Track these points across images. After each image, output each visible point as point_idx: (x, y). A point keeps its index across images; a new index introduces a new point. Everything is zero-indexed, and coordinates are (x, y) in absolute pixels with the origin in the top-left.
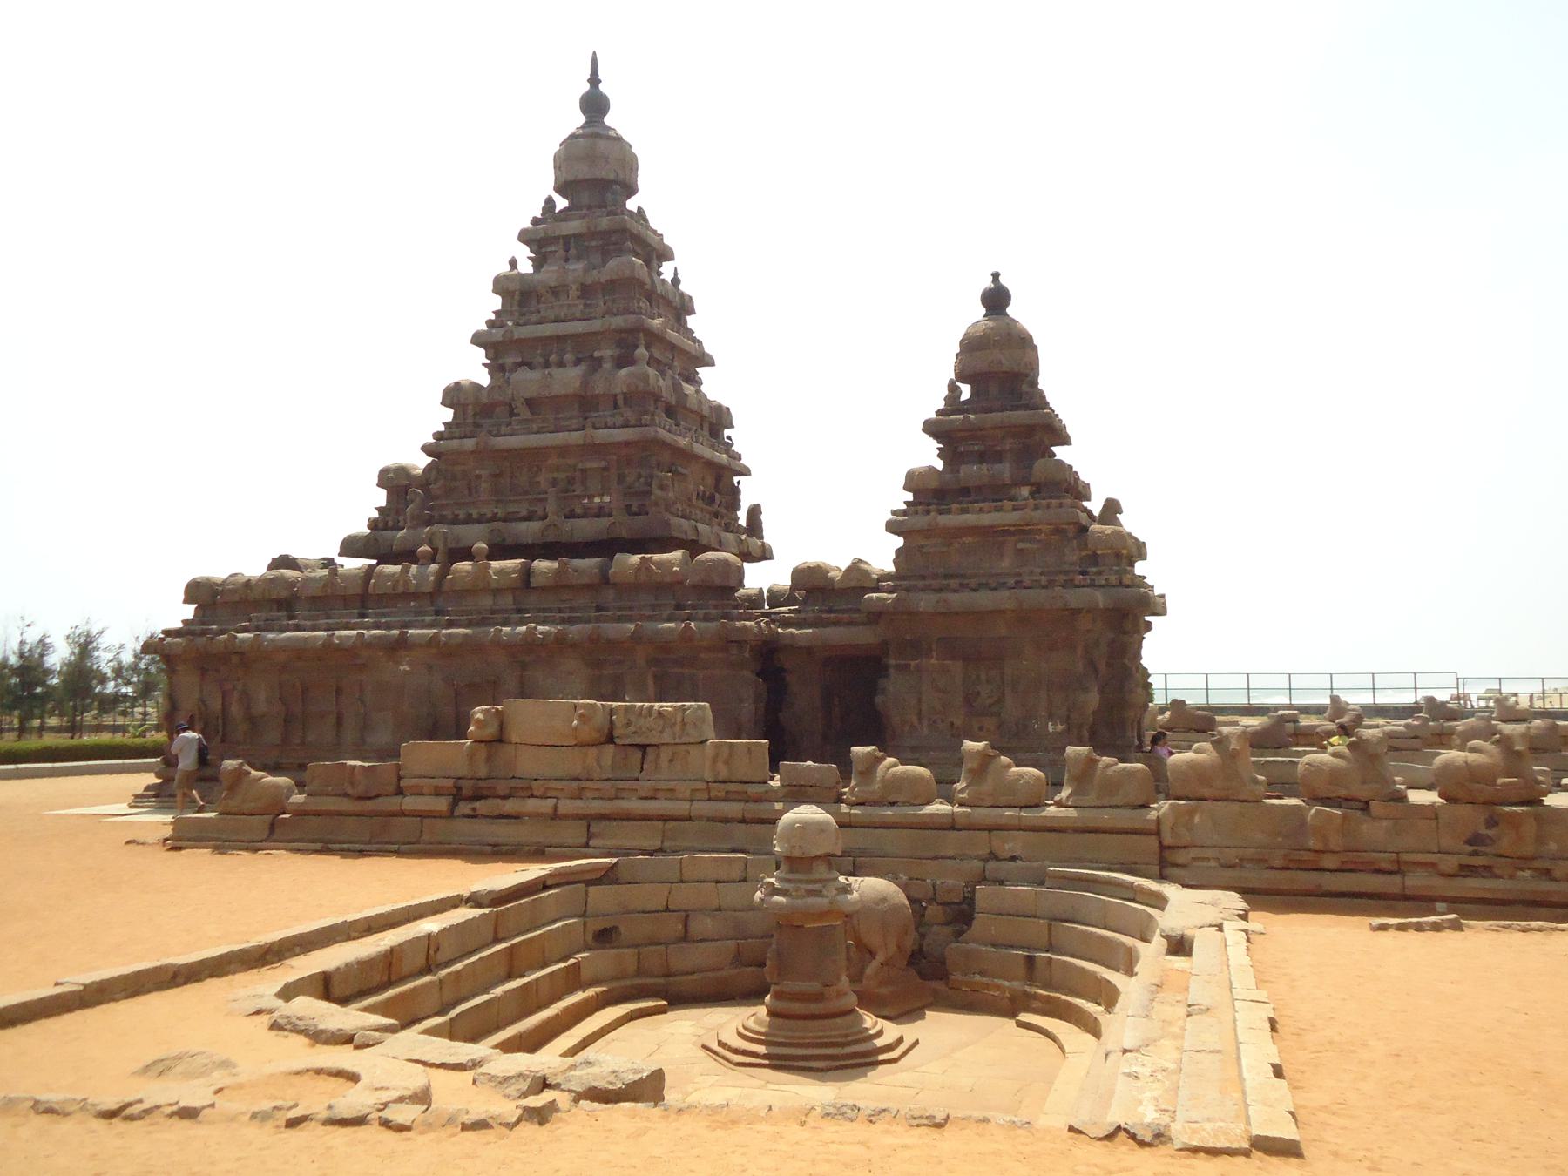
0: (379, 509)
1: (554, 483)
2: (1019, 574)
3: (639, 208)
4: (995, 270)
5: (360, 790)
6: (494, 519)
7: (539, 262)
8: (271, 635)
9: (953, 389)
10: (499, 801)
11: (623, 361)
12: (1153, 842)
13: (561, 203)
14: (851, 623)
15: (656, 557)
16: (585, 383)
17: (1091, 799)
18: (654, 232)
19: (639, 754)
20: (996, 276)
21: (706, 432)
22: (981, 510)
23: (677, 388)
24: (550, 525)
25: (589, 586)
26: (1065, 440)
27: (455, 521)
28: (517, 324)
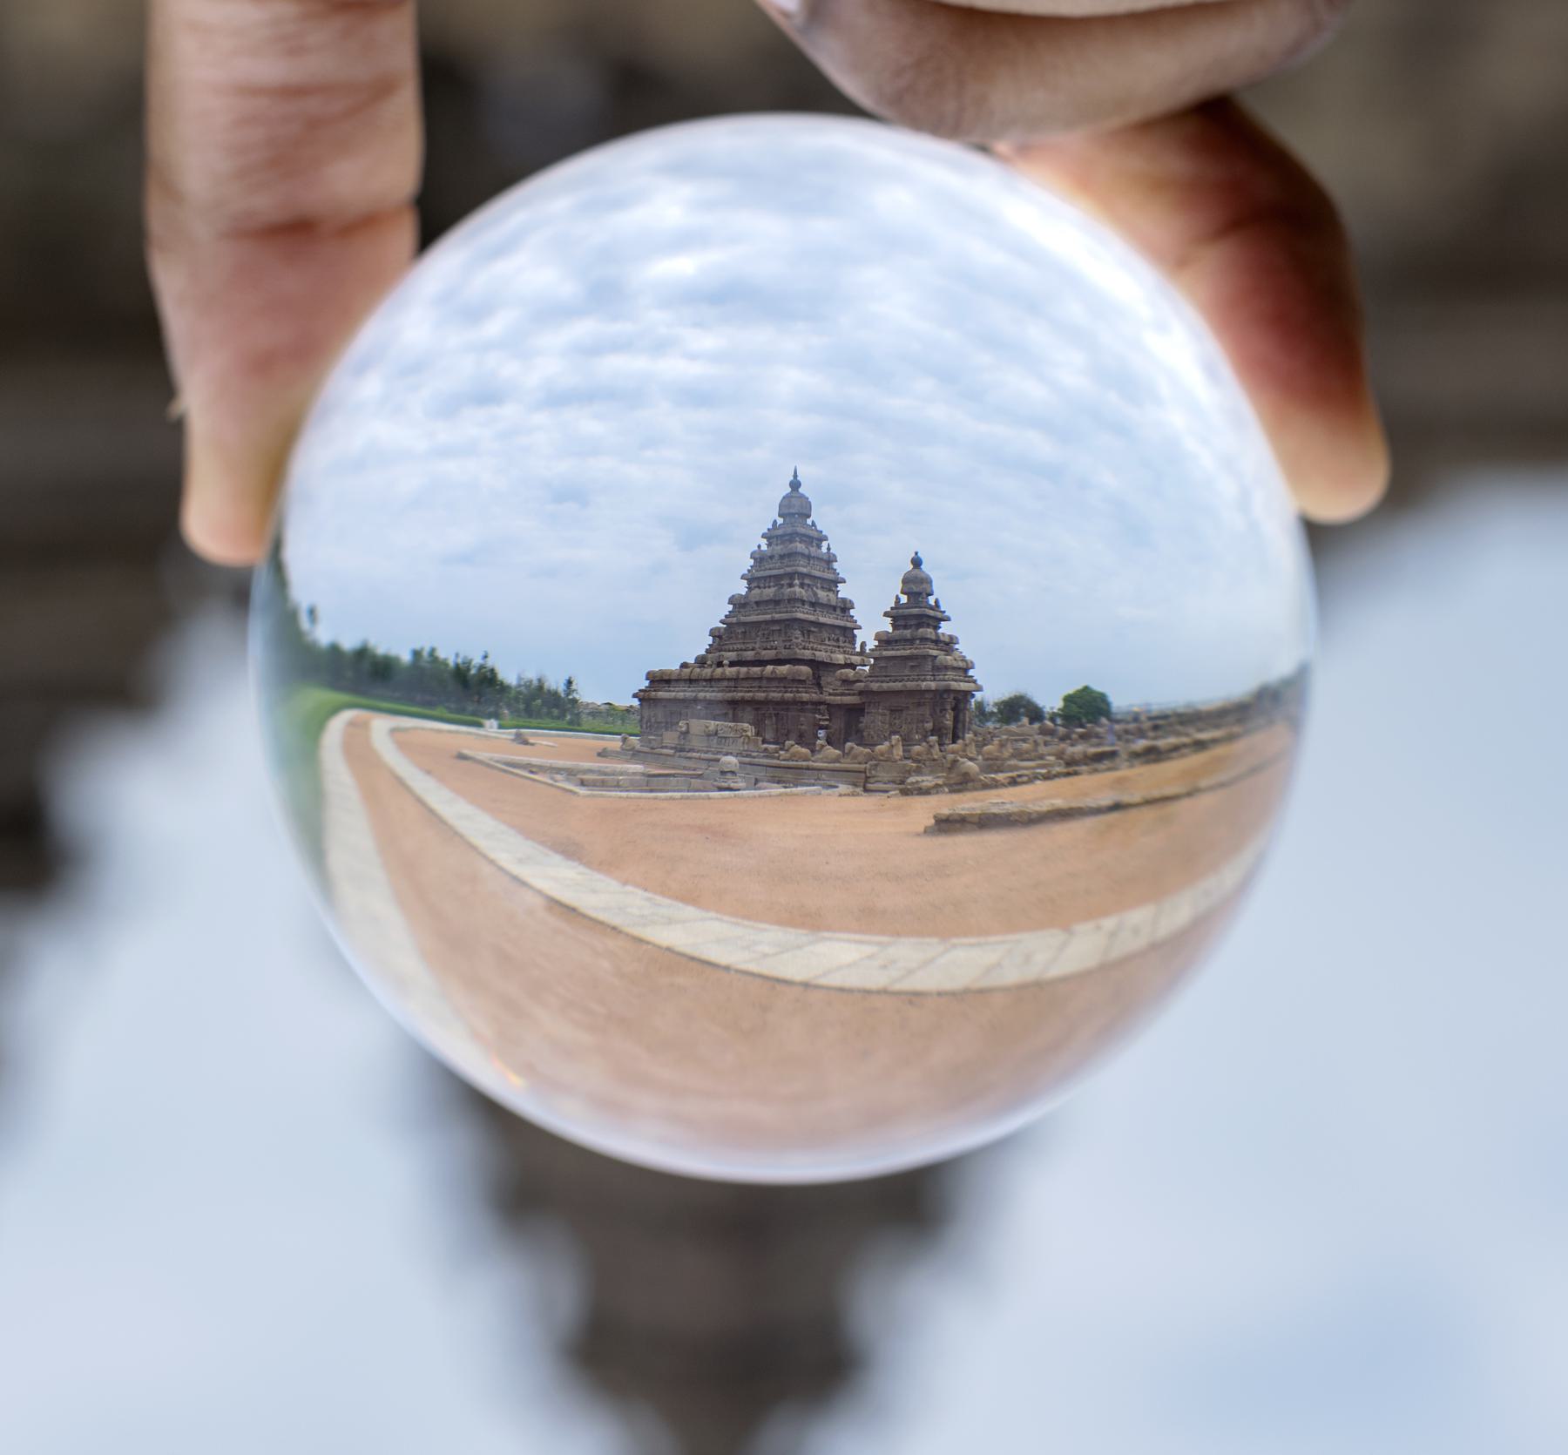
0: (709, 645)
1: (764, 634)
2: (909, 676)
3: (813, 522)
4: (917, 550)
5: (651, 745)
6: (741, 650)
7: (769, 545)
8: (660, 693)
9: (897, 598)
10: (685, 753)
11: (791, 585)
12: (863, 775)
13: (780, 521)
14: (854, 695)
15: (779, 667)
16: (775, 595)
17: (849, 760)
18: (817, 531)
19: (723, 741)
20: (916, 553)
21: (838, 612)
22: (898, 650)
23: (815, 594)
24: (756, 654)
25: (758, 678)
26: (948, 619)
27: (729, 651)
28: (757, 571)
